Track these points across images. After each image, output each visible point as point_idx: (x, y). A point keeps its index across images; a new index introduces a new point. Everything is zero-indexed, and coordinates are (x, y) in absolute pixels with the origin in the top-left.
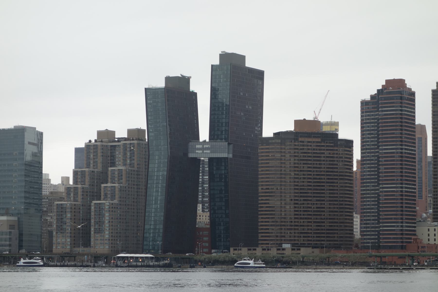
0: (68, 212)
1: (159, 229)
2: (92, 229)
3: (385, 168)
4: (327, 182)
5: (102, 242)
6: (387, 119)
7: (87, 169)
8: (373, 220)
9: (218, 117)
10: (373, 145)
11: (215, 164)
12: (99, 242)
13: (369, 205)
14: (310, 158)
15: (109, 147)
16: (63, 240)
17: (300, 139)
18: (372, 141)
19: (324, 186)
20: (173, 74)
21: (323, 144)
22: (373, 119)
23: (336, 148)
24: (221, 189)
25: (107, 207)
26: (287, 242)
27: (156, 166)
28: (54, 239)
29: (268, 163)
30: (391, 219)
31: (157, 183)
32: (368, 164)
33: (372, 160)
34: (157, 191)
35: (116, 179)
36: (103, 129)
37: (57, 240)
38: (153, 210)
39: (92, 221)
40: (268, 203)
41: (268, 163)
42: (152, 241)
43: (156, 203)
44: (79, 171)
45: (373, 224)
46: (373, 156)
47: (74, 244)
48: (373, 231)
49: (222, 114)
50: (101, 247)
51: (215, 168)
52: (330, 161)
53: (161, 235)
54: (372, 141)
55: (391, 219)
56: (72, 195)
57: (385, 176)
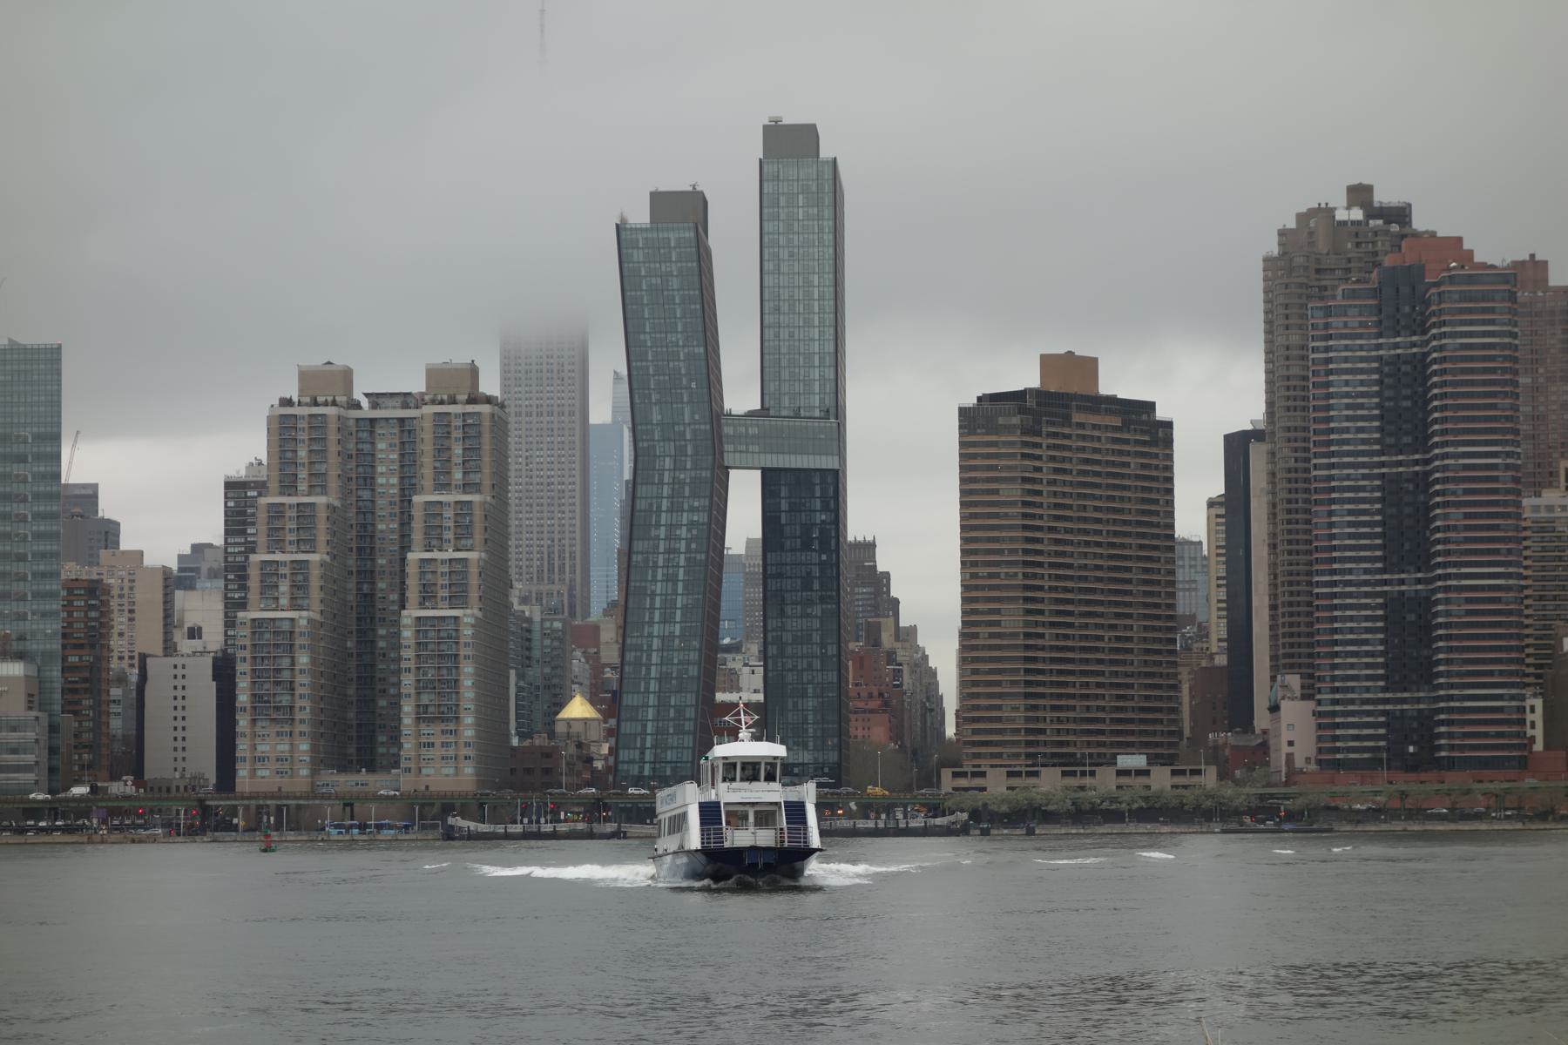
0: (301, 647)
1: (680, 710)
2: (408, 708)
3: (1467, 516)
4: (1140, 558)
5: (451, 752)
6: (1472, 359)
7: (320, 500)
8: (1368, 678)
9: (791, 335)
10: (1364, 441)
11: (784, 492)
12: (437, 752)
13: (1351, 631)
15: (352, 423)
16: (281, 748)
17: (1077, 417)
18: (1360, 430)
19: (1128, 569)
20: (664, 187)
21: (1126, 436)
22: (1362, 360)
23: (1154, 450)
24: (809, 574)
25: (469, 632)
26: (1129, 747)
27: (666, 491)
28: (242, 746)
29: (996, 492)
30: (1491, 673)
31: (669, 551)
32: (1350, 501)
33: (1362, 489)
34: (671, 579)
35: (448, 535)
36: (316, 361)
37: (254, 747)
38: (656, 643)
39: (408, 680)
40: (998, 624)
41: (996, 492)
42: (654, 747)
43: (667, 619)
44: (291, 506)
45: (1368, 690)
46: (1364, 477)
48: (1369, 713)
49: (808, 324)
50: (445, 771)
51: (784, 505)
52: (1144, 489)
53: (689, 726)
54: (1360, 430)
55: (1491, 673)
56: (284, 587)
57: (1467, 540)
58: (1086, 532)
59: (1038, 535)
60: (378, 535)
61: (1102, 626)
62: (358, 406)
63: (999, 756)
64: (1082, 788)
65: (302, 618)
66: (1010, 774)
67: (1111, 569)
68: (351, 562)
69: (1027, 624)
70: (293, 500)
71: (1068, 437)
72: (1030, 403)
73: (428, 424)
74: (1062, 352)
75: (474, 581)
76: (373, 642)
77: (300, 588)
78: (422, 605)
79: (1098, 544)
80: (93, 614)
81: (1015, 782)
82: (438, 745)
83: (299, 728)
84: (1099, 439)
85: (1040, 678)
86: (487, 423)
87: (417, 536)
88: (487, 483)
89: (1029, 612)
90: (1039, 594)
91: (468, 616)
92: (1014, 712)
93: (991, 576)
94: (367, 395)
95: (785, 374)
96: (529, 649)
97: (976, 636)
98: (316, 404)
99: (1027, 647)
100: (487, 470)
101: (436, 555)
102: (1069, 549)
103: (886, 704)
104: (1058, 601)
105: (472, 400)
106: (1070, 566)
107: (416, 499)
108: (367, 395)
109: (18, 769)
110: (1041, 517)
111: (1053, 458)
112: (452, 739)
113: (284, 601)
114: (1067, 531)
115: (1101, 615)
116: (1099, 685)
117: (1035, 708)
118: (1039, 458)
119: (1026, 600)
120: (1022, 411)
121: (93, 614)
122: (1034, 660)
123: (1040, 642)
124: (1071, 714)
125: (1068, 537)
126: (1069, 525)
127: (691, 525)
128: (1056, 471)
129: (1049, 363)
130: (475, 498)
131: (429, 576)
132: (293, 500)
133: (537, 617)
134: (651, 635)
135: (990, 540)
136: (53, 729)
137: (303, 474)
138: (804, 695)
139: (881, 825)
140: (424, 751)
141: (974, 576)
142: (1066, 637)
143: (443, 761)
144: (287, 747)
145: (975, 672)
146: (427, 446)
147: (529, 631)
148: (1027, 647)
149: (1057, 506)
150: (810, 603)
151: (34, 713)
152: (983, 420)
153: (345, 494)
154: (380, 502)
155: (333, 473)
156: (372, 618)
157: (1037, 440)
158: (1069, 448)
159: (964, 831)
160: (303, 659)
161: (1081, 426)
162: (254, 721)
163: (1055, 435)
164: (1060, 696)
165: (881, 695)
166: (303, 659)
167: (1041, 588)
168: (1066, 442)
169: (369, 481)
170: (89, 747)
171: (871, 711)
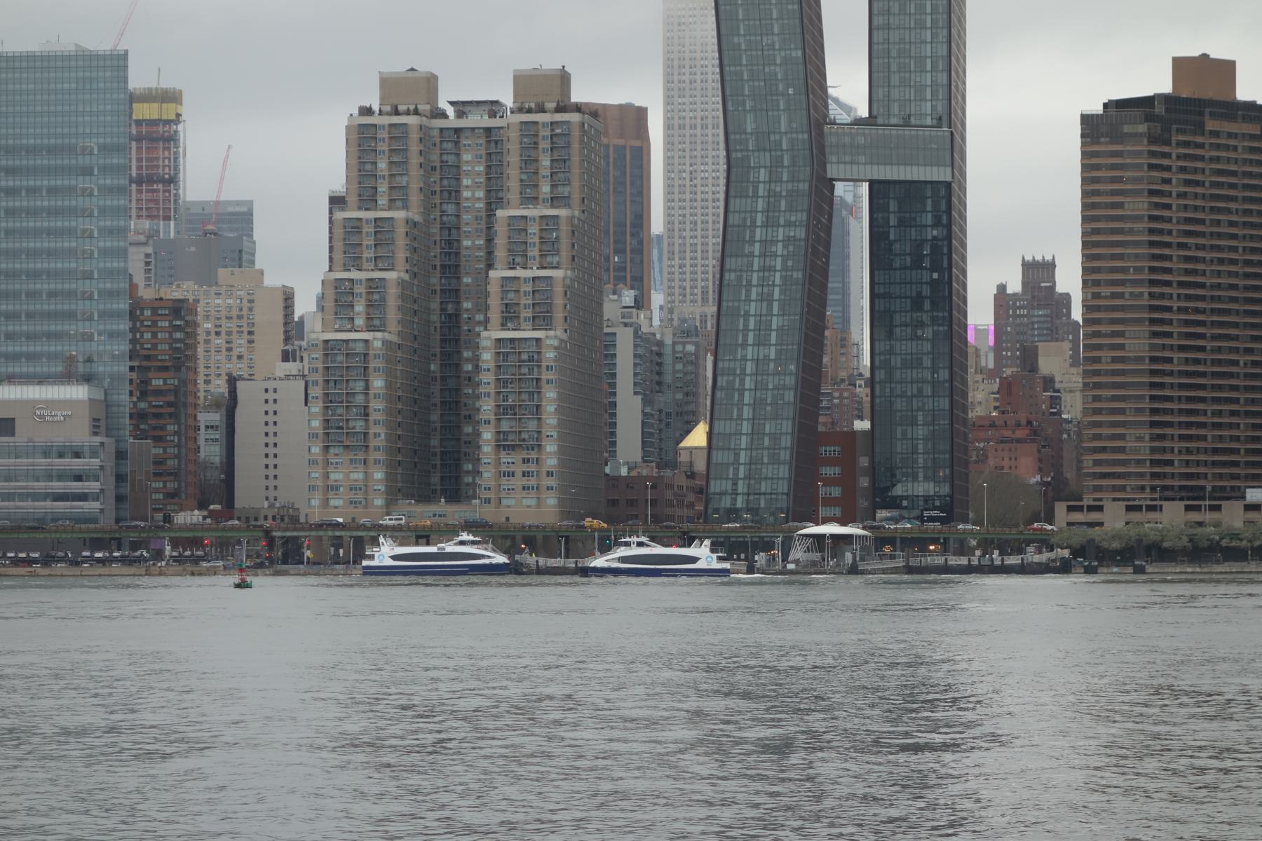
1: (775, 437)
2: (487, 435)
5: (532, 482)
7: (399, 215)
11: (893, 206)
12: (518, 482)
14: (1233, 193)
15: (435, 133)
16: (354, 476)
17: (1211, 125)
24: (919, 294)
25: (551, 355)
27: (761, 204)
29: (1120, 205)
31: (763, 269)
34: (766, 299)
35: (534, 252)
36: (398, 67)
38: (750, 367)
39: (487, 407)
40: (1121, 347)
41: (1120, 205)
42: (748, 477)
44: (367, 221)
47: (394, 494)
49: (921, 26)
51: (893, 220)
53: (785, 455)
56: (360, 308)
58: (1219, 249)
59: (1167, 252)
60: (464, 252)
61: (1237, 350)
62: (444, 115)
63: (1123, 488)
64: (1200, 524)
65: (377, 340)
66: (1129, 509)
67: (1246, 288)
68: (435, 280)
69: (1153, 347)
70: (370, 215)
71: (1202, 146)
72: (1159, 109)
73: (514, 135)
74: (1196, 54)
75: (559, 301)
76: (458, 365)
77: (375, 307)
78: (504, 326)
79: (1233, 262)
80: (178, 335)
81: (1135, 516)
82: (519, 474)
83: (374, 455)
84: (1235, 148)
85: (1168, 405)
86: (576, 133)
87: (501, 253)
88: (576, 196)
89: (1155, 334)
90: (1167, 316)
91: (551, 338)
92: (1138, 443)
93: (1114, 296)
94: (452, 103)
95: (895, 79)
96: (659, 374)
97: (1097, 360)
98: (397, 113)
99: (1153, 373)
100: (576, 183)
101: (519, 273)
102: (1200, 267)
103: (1035, 433)
104: (1187, 323)
105: (559, 109)
106: (1202, 286)
107: (499, 213)
108: (452, 103)
109: (83, 497)
110: (1170, 232)
111: (1183, 169)
112: (532, 467)
113: (360, 322)
114: (1198, 247)
115: (1236, 338)
116: (1233, 413)
117: (1162, 437)
118: (1168, 168)
119: (1153, 321)
120: (1149, 118)
121: (178, 335)
122: (1161, 386)
123: (1167, 367)
124: (1202, 445)
125: (1200, 254)
126: (1200, 241)
127: (788, 240)
128: (1188, 183)
129: (1181, 66)
130: (562, 212)
131: (511, 295)
132: (370, 215)
133: (668, 341)
134: (744, 359)
135: (1114, 257)
136: (120, 455)
137: (383, 188)
138: (914, 423)
139: (975, 562)
140: (504, 481)
141: (1096, 296)
142: (1197, 362)
143: (526, 492)
144: (361, 476)
145: (1096, 399)
146: (513, 158)
147: (659, 355)
148: (1153, 373)
149: (1188, 221)
150: (921, 324)
151: (98, 439)
152: (1107, 129)
153: (428, 208)
154: (466, 217)
155: (415, 186)
156: (457, 341)
157: (1166, 149)
158: (1202, 158)
159: (1064, 568)
160: (378, 383)
161: (1216, 134)
162: (326, 448)
163: (1186, 144)
164: (1189, 425)
165: (1029, 423)
166: (378, 383)
167: (1169, 309)
168: (1199, 152)
169: (454, 194)
170: (175, 474)
171: (1019, 441)
